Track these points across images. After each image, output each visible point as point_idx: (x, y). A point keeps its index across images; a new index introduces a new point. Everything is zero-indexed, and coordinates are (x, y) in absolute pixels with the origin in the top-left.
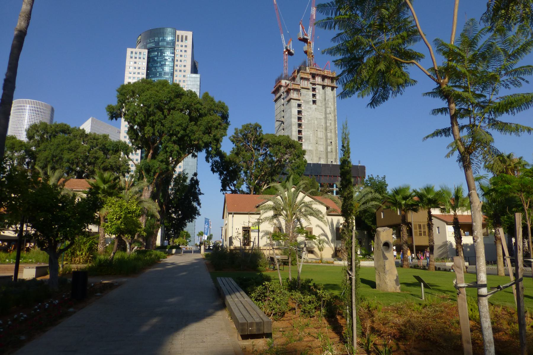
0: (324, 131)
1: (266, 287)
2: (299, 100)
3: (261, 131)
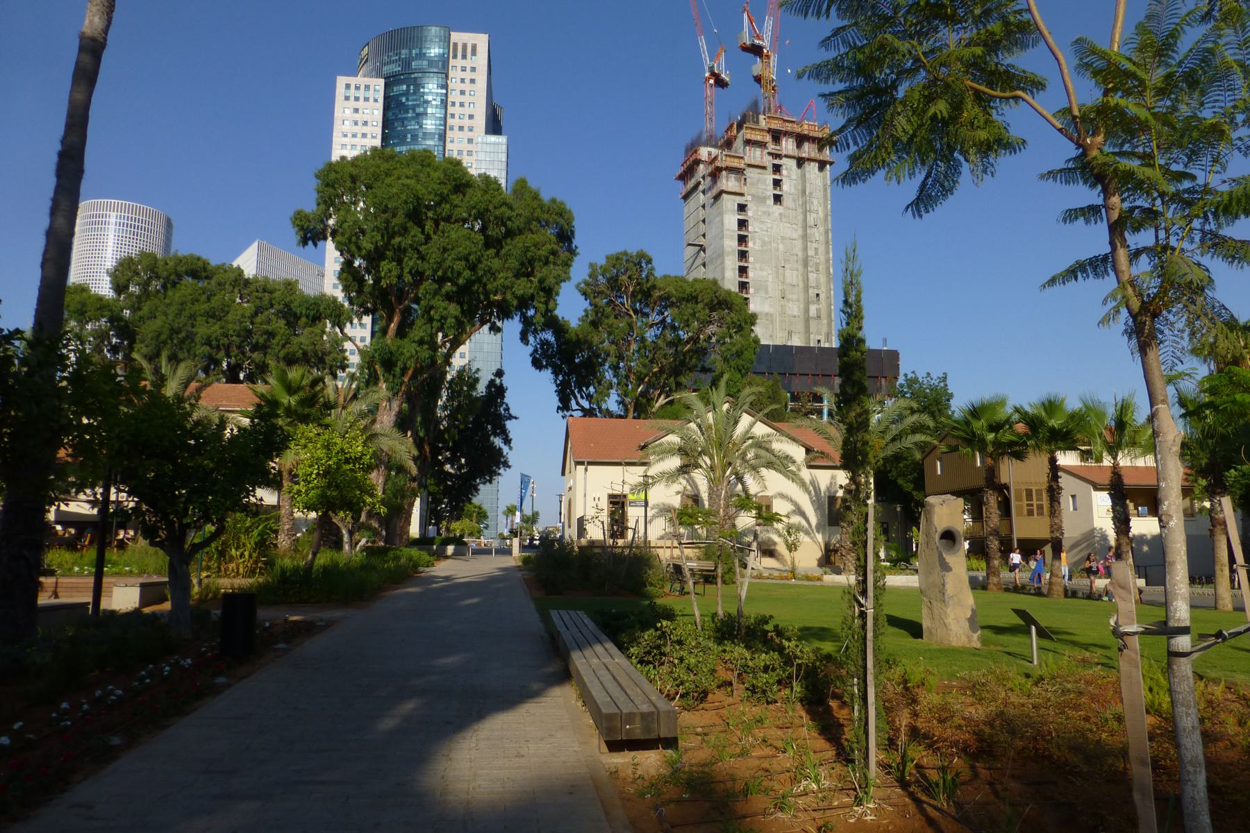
0: (800, 268)
1: (664, 633)
2: (742, 195)
3: (653, 269)
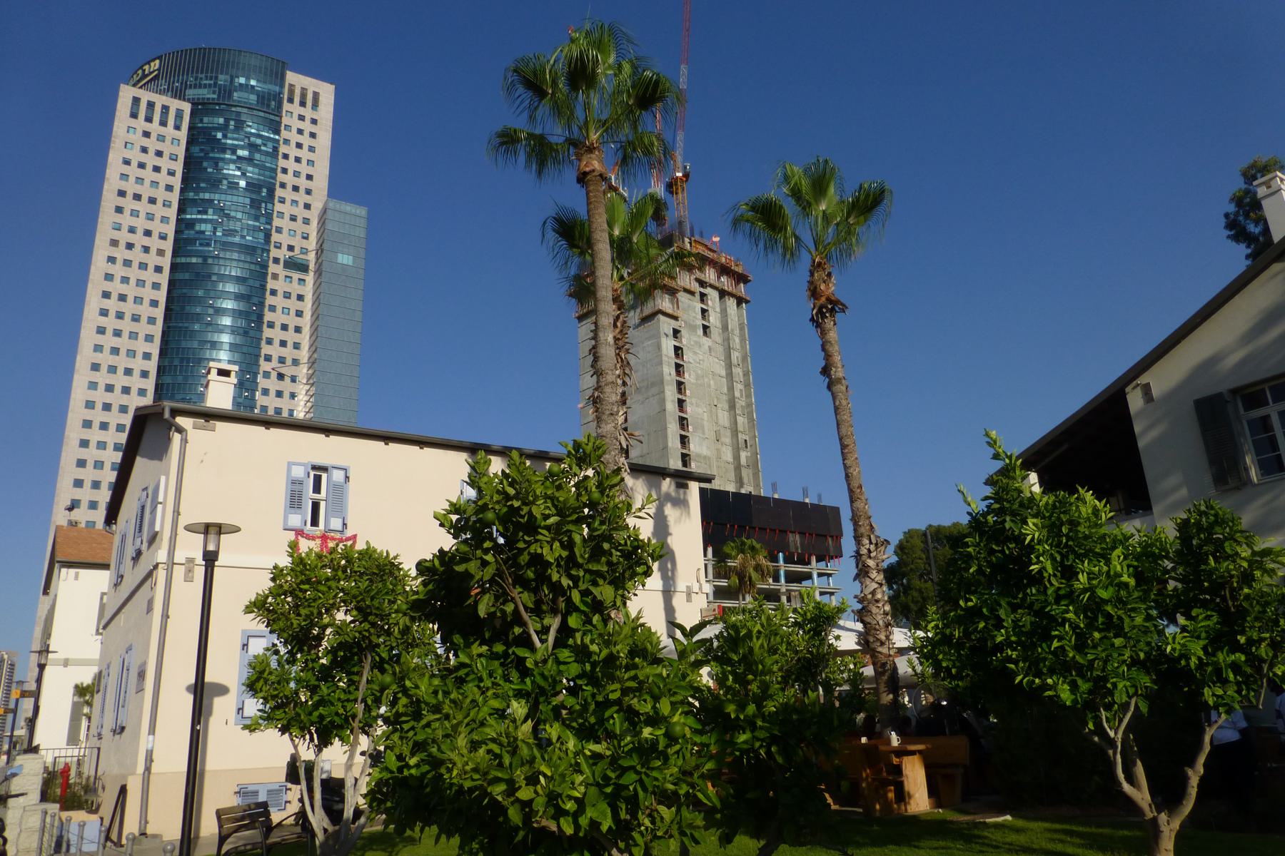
2: (676, 318)
